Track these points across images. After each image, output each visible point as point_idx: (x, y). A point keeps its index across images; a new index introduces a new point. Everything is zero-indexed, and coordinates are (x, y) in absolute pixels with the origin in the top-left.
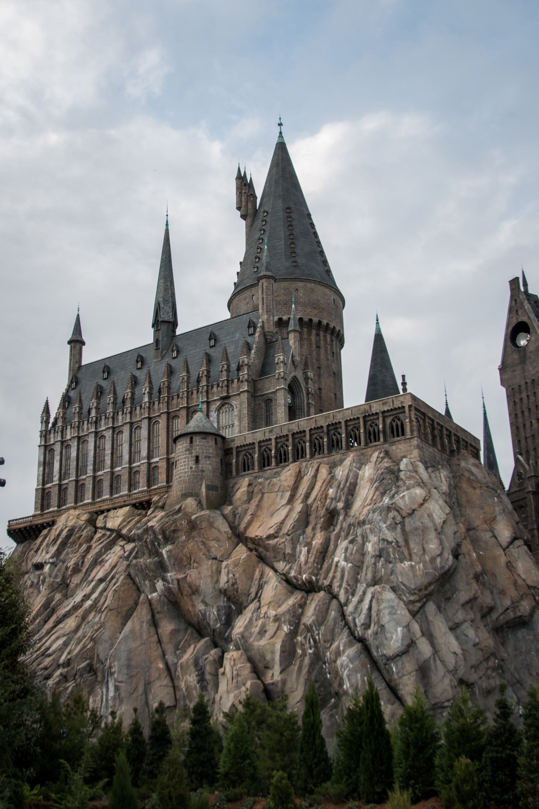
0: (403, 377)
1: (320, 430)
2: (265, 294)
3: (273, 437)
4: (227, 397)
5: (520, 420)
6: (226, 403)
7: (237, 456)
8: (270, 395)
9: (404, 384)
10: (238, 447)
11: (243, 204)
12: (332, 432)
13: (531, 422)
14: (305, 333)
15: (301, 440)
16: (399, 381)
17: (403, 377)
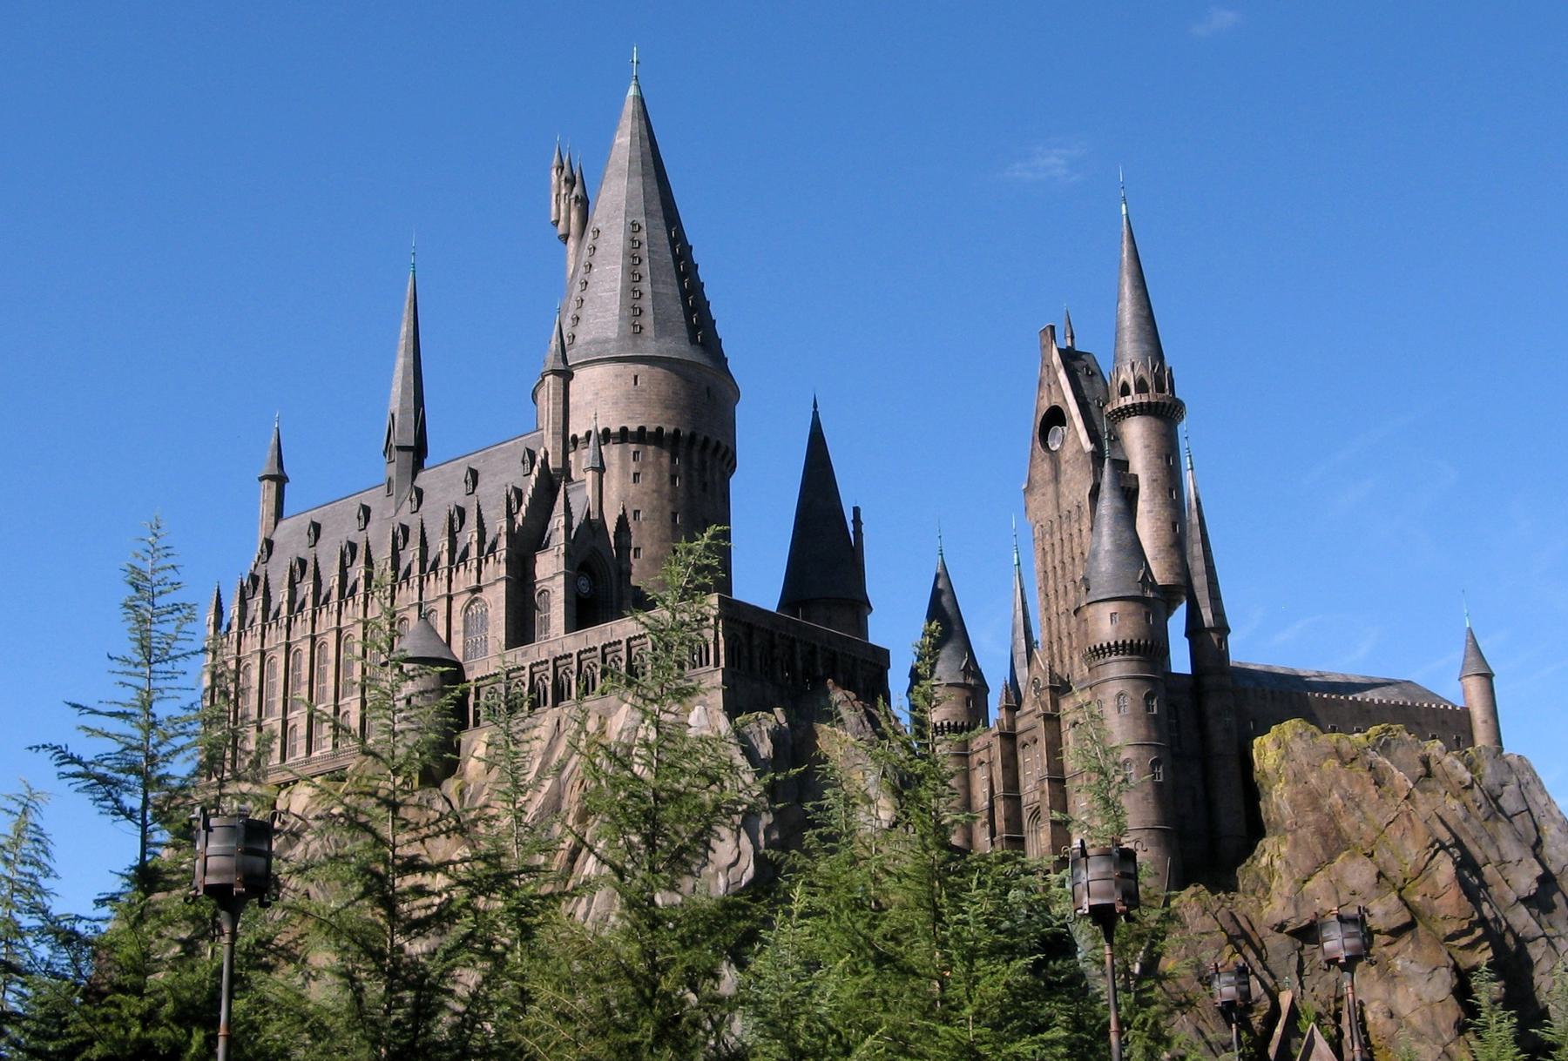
0: (856, 511)
1: (593, 653)
2: (551, 402)
3: (527, 665)
4: (478, 589)
5: (1051, 582)
6: (476, 599)
7: (477, 696)
8: (546, 583)
9: (857, 521)
10: (477, 680)
11: (562, 215)
12: (609, 658)
13: (1066, 587)
14: (651, 454)
15: (567, 668)
16: (849, 517)
17: (856, 511)
